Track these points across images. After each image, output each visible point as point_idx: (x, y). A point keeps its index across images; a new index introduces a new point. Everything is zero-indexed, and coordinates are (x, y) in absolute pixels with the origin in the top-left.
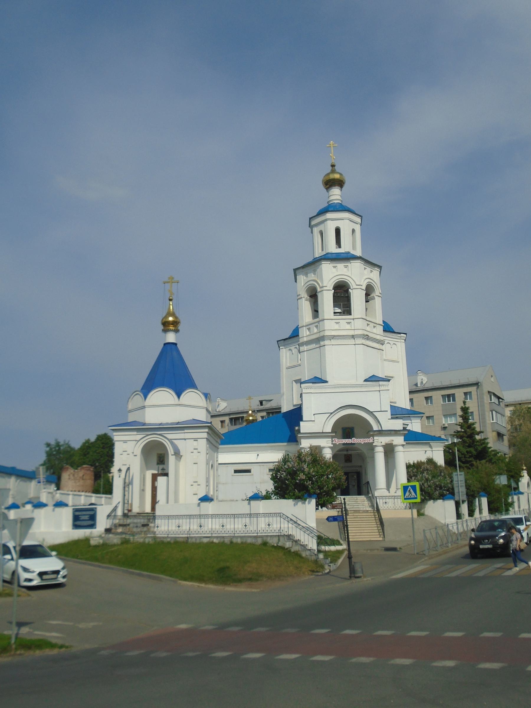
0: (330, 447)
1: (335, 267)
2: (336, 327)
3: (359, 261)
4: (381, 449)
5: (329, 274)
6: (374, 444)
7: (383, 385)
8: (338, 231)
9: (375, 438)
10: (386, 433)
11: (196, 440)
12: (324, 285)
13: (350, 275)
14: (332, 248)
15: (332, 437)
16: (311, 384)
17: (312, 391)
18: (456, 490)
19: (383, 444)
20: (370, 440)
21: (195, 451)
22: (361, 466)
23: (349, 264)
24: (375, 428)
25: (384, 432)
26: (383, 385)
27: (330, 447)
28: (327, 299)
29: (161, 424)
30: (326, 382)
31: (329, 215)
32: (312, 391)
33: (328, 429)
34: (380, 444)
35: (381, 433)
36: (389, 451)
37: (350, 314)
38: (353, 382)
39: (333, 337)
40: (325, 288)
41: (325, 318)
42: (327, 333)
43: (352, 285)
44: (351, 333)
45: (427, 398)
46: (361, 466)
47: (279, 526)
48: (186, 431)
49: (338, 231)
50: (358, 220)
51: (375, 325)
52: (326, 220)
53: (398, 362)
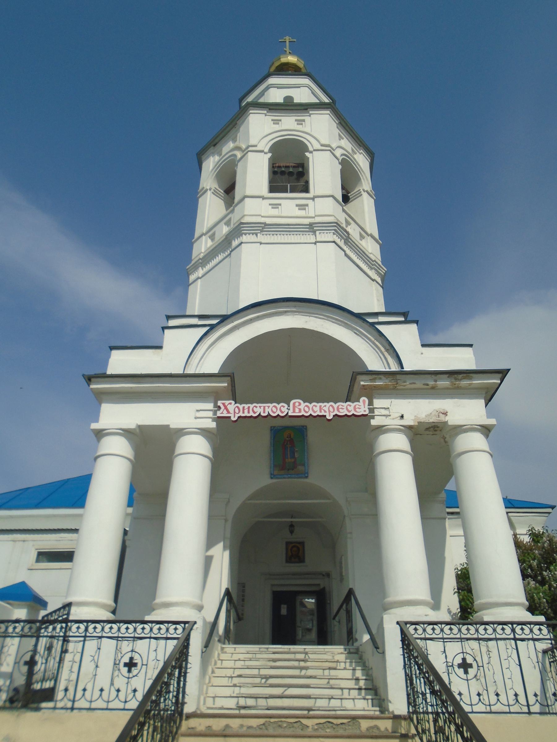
0: (204, 432)
2: (275, 212)
3: (328, 112)
4: (400, 441)
6: (373, 422)
9: (377, 403)
10: (419, 383)
13: (309, 131)
15: (215, 396)
19: (409, 421)
20: (360, 407)
22: (328, 575)
23: (307, 119)
25: (408, 383)
27: (204, 432)
31: (272, 80)
34: (395, 422)
35: (401, 381)
37: (306, 189)
39: (264, 228)
40: (250, 149)
43: (312, 144)
46: (328, 575)
52: (268, 88)
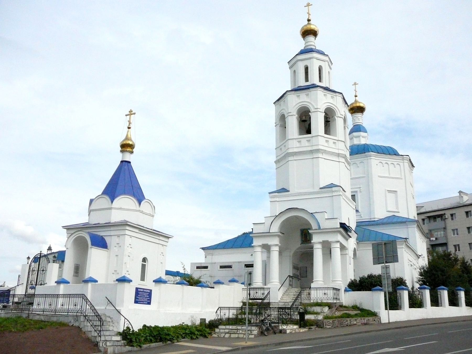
1: (298, 96)
5: (294, 103)
7: (336, 191)
8: (307, 69)
11: (118, 236)
12: (290, 111)
14: (302, 83)
16: (276, 194)
17: (277, 199)
18: (383, 283)
21: (130, 246)
24: (314, 226)
26: (336, 191)
28: (293, 123)
29: (99, 224)
30: (289, 191)
32: (277, 199)
33: (275, 228)
36: (327, 248)
38: (312, 190)
41: (289, 138)
42: (290, 151)
43: (312, 109)
44: (309, 149)
45: (467, 213)
47: (67, 307)
48: (112, 229)
49: (307, 69)
50: (326, 58)
51: (335, 141)
53: (401, 179)
